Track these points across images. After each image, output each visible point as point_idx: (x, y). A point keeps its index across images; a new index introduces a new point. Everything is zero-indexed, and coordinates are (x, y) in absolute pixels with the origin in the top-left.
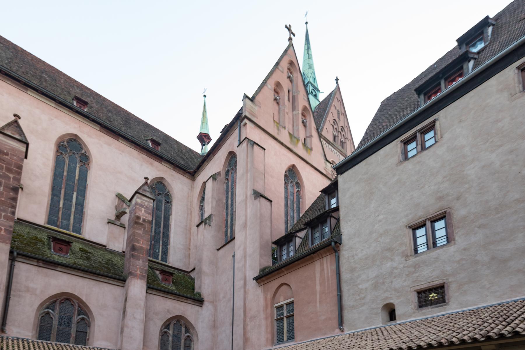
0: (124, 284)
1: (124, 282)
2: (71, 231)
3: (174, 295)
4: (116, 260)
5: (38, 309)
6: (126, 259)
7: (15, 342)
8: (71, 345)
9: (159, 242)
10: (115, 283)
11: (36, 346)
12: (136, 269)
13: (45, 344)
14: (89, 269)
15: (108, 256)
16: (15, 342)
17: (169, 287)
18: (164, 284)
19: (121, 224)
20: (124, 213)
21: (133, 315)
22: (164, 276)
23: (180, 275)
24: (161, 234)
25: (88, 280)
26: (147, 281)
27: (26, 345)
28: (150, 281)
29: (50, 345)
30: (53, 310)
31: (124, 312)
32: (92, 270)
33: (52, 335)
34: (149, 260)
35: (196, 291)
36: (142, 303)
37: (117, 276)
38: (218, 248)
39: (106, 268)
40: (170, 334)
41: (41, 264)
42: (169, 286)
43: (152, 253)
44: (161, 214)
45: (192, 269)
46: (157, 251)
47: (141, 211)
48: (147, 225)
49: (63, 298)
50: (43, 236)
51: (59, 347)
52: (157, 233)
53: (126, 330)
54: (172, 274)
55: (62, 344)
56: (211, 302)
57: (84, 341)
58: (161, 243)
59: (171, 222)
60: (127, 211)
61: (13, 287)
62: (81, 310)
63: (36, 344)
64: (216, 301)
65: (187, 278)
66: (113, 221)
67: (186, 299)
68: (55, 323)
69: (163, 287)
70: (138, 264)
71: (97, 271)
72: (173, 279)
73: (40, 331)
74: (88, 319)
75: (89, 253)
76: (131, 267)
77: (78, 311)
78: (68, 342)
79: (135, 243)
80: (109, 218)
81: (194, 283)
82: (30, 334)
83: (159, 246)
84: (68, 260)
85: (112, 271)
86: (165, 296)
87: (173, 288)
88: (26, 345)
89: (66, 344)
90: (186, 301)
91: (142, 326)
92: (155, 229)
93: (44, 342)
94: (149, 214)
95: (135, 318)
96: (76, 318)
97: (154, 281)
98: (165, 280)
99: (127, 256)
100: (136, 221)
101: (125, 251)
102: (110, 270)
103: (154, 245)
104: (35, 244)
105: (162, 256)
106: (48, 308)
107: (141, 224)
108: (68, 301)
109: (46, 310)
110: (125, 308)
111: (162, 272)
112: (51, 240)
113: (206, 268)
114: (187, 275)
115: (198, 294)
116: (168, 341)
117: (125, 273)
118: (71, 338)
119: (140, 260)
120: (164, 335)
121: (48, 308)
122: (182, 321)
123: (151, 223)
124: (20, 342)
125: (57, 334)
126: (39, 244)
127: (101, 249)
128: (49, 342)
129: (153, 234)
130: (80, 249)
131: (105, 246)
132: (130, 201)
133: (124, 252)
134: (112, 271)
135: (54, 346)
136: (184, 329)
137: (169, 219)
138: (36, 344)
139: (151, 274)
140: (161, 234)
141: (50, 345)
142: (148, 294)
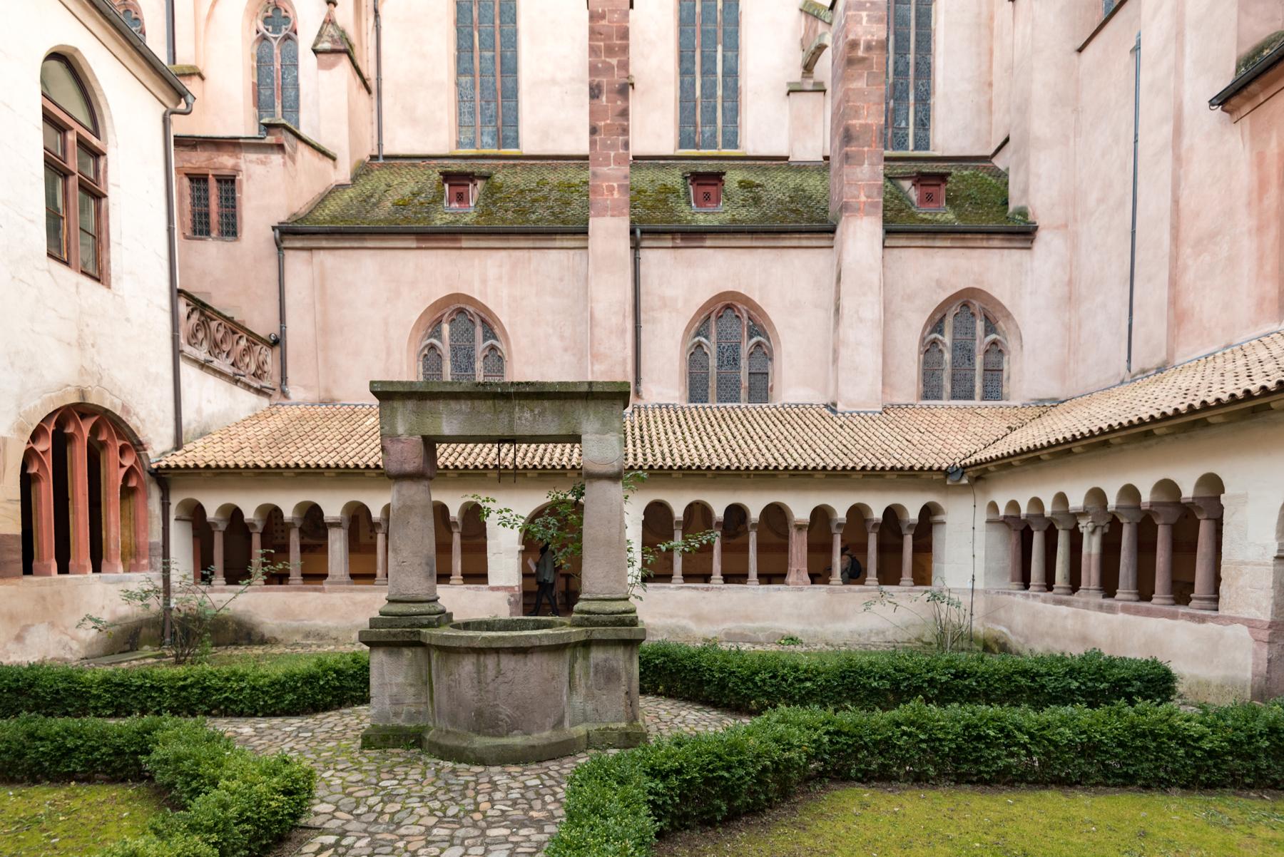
0: (833, 238)
1: (831, 235)
2: (720, 146)
3: (952, 236)
4: (812, 183)
5: (684, 342)
6: (832, 173)
7: (657, 411)
8: (743, 406)
9: (908, 98)
10: (814, 243)
11: (688, 416)
12: (856, 193)
13: (701, 410)
14: (760, 226)
15: (794, 180)
16: (657, 411)
17: (938, 217)
18: (926, 214)
19: (815, 84)
20: (821, 48)
21: (857, 312)
22: (924, 188)
23: (965, 173)
24: (912, 72)
25: (760, 251)
26: (884, 215)
27: (673, 416)
28: (889, 214)
29: (708, 410)
30: (706, 337)
31: (837, 310)
32: (767, 225)
33: (710, 391)
34: (887, 159)
35: (1012, 207)
36: (875, 278)
37: (816, 225)
38: (1079, 44)
39: (793, 211)
40: (944, 344)
41: (679, 242)
42: (936, 214)
43: (890, 135)
44: (909, 10)
45: (999, 144)
46: (903, 125)
47: (860, 22)
48: (875, 57)
49: (720, 306)
50: (674, 178)
51: (724, 412)
52: (900, 72)
53: (843, 352)
54: (943, 177)
55: (728, 405)
56: (1057, 228)
57: (764, 394)
58: (912, 97)
59: (935, 24)
60: (828, 40)
61: (643, 305)
62: (755, 325)
63: (687, 412)
64: (1076, 220)
65: (986, 176)
66: (798, 83)
67: (985, 236)
68: (713, 362)
69: (923, 220)
70: (860, 175)
71: (777, 225)
72: (947, 190)
73: (691, 384)
74: (767, 343)
75: (758, 186)
76: (846, 189)
77: (749, 327)
78: (737, 400)
79: (850, 122)
80: (789, 80)
81: (1007, 184)
82: (677, 394)
83: (908, 109)
84: (721, 217)
85: (805, 216)
86: (930, 243)
87: (947, 216)
88: (673, 416)
89: (735, 405)
90: (985, 244)
91: (878, 337)
92: (895, 63)
93: (699, 405)
94: (880, 20)
95: (861, 320)
96: (746, 346)
97: (901, 211)
98: (928, 199)
99: (835, 163)
100: (851, 60)
101: (827, 153)
102: (801, 213)
103: (894, 110)
104: (665, 201)
105: (915, 135)
106: (698, 334)
107: (863, 60)
108: (729, 311)
109: (696, 339)
110: (838, 298)
111: (921, 179)
112: (689, 181)
113: (1041, 125)
114: (985, 167)
115: (1020, 214)
116: (940, 363)
117: (833, 209)
118: (742, 391)
119: (862, 164)
120: (930, 348)
121: (698, 334)
122: (974, 302)
123: (883, 45)
124: (664, 411)
125: (718, 387)
126: (672, 198)
127: (778, 168)
128: (706, 405)
129: (891, 80)
130: (740, 182)
131: (786, 158)
132: (832, 7)
133: (826, 158)
134: (805, 216)
135: (716, 410)
136: (983, 323)
137: (929, 17)
138: (687, 412)
139: (892, 194)
140: (912, 72)
141: (708, 410)
142: (887, 250)
